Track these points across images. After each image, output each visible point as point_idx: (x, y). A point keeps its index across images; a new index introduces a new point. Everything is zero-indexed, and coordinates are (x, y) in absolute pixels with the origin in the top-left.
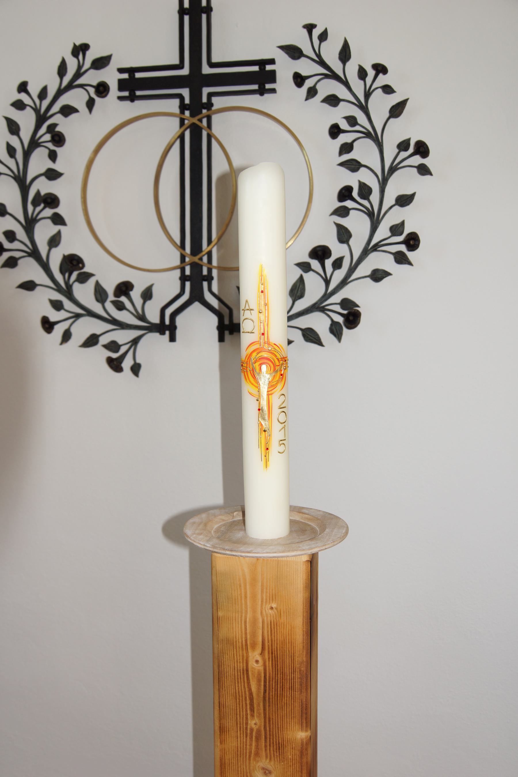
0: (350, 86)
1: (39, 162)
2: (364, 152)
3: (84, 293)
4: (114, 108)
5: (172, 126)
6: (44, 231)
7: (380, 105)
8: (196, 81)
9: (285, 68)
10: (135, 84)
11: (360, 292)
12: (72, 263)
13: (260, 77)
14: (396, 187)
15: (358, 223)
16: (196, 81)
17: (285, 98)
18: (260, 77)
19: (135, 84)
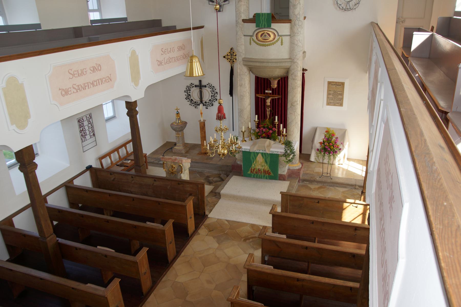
0: (212, 87)
1: (189, 92)
2: (213, 92)
3: (193, 102)
4: (194, 88)
5: (199, 90)
6: (189, 97)
7: (214, 89)
8: (200, 86)
9: (207, 86)
10: (196, 86)
11: (213, 103)
12: (192, 100)
13: (205, 86)
14: (216, 95)
15: (213, 98)
16: (200, 86)
17: (207, 88)
18: (205, 86)
19: (196, 86)
